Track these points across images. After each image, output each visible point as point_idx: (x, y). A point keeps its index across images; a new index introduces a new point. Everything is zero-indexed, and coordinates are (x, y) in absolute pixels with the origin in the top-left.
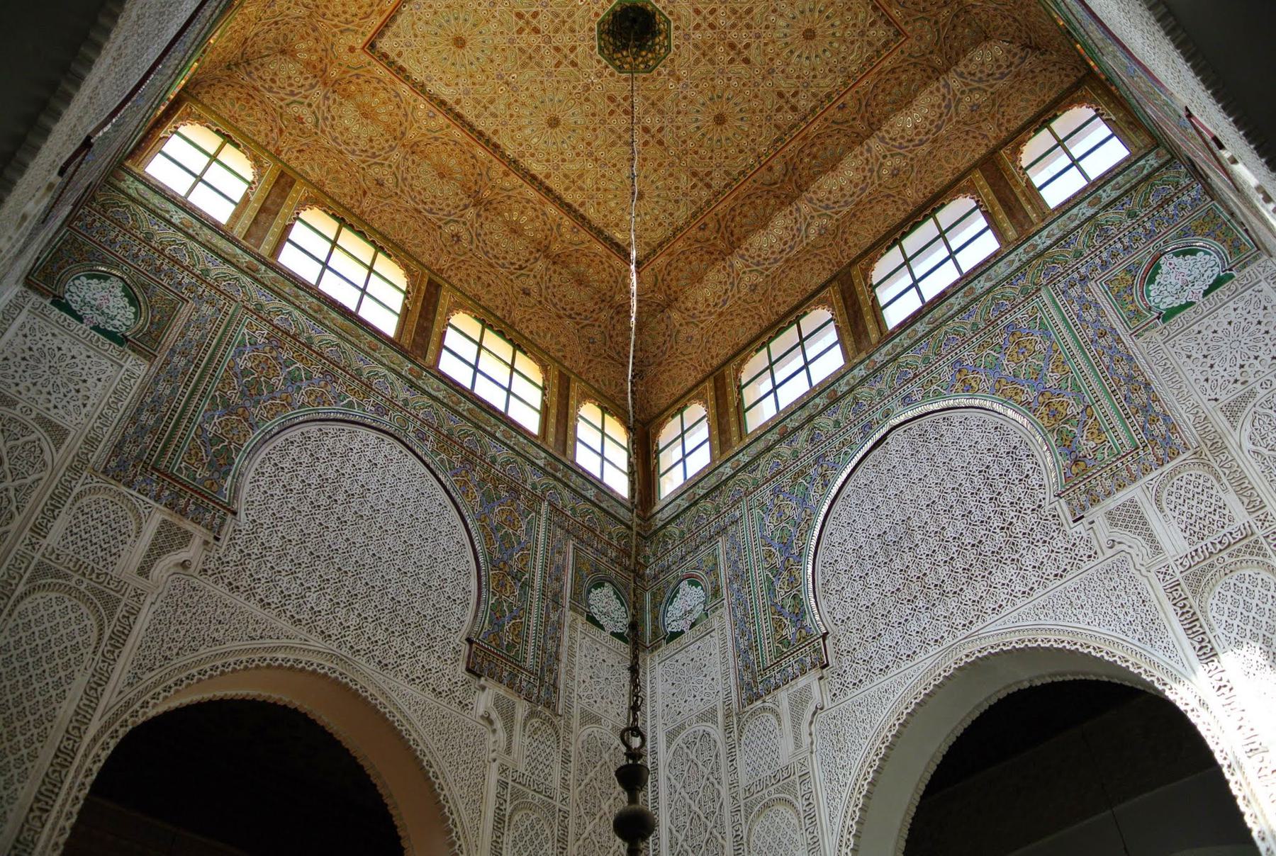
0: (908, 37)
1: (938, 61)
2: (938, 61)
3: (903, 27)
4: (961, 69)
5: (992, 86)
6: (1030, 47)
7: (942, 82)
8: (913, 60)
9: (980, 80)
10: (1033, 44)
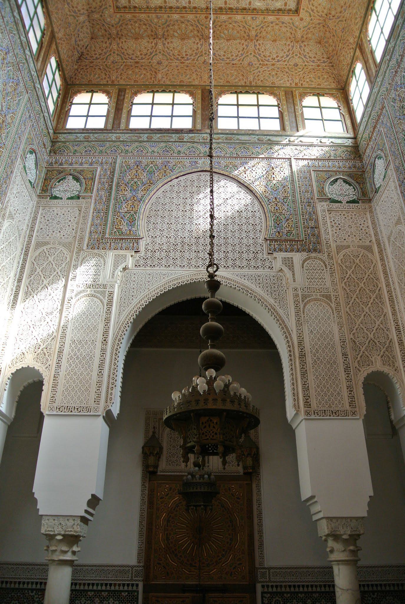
0: (115, 12)
1: (96, 16)
2: (96, 16)
3: (120, 14)
4: (87, 23)
5: (74, 35)
6: (81, 56)
7: (86, 12)
8: (103, 7)
9: (79, 31)
10: (82, 58)
